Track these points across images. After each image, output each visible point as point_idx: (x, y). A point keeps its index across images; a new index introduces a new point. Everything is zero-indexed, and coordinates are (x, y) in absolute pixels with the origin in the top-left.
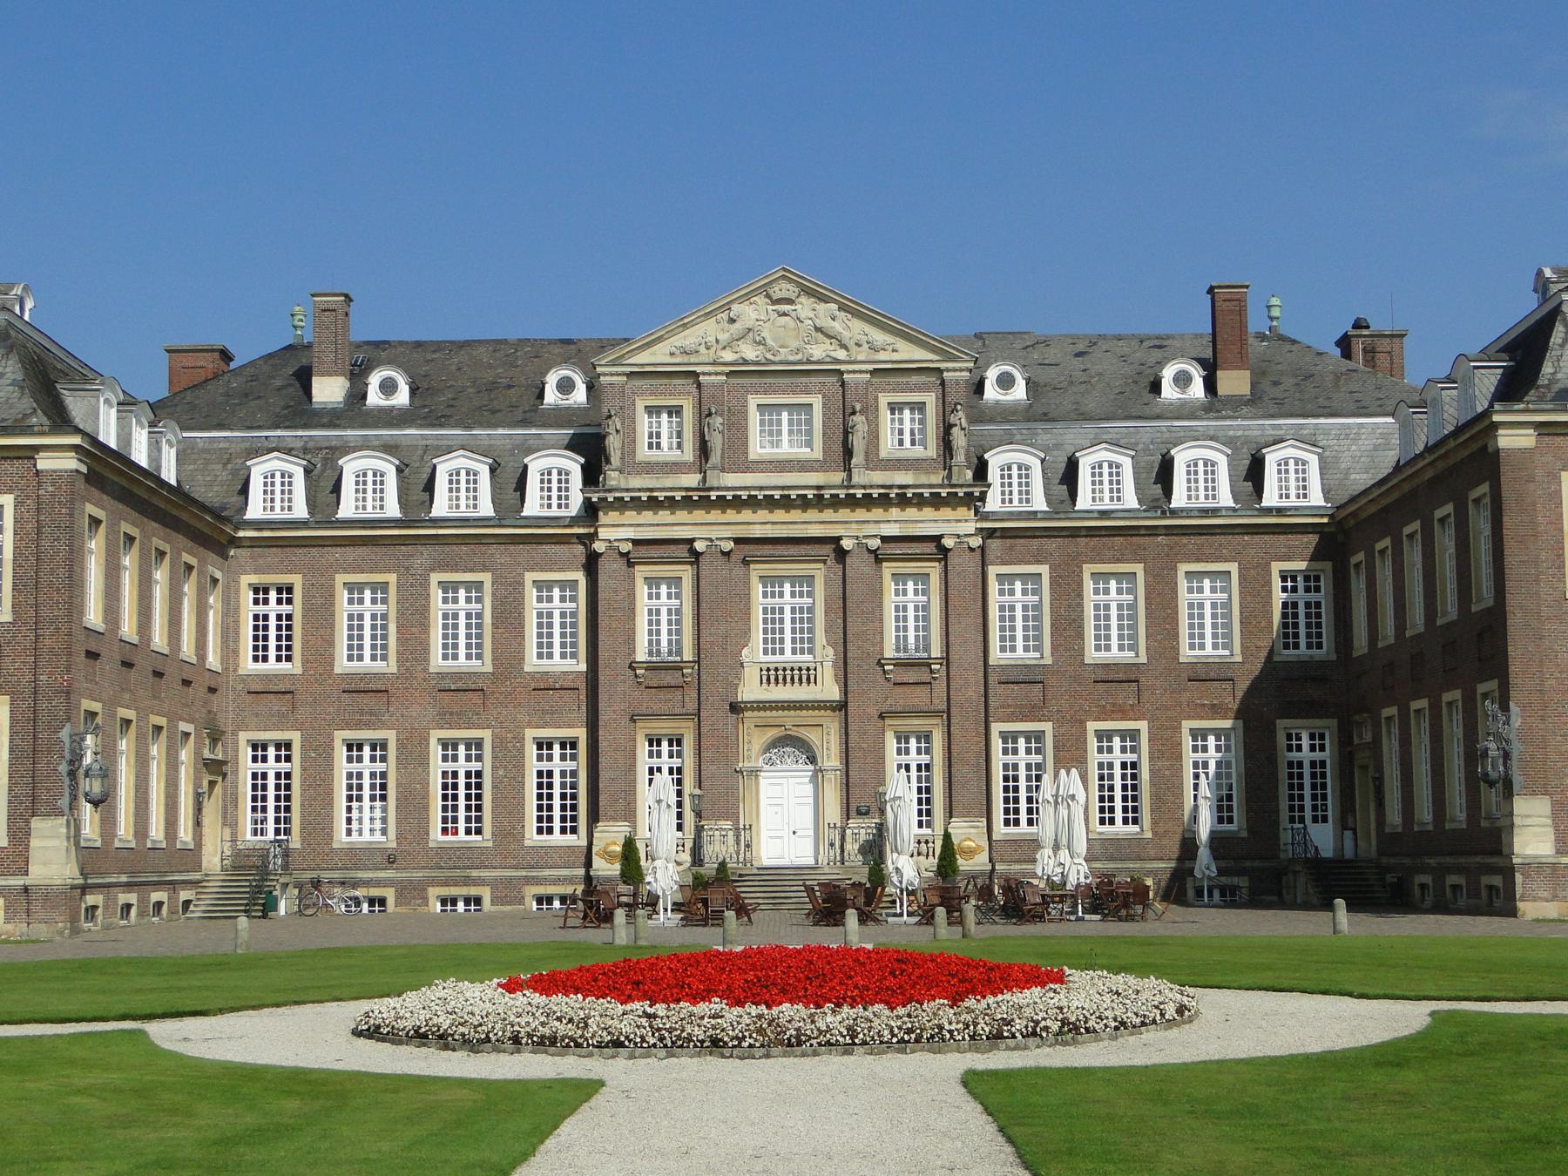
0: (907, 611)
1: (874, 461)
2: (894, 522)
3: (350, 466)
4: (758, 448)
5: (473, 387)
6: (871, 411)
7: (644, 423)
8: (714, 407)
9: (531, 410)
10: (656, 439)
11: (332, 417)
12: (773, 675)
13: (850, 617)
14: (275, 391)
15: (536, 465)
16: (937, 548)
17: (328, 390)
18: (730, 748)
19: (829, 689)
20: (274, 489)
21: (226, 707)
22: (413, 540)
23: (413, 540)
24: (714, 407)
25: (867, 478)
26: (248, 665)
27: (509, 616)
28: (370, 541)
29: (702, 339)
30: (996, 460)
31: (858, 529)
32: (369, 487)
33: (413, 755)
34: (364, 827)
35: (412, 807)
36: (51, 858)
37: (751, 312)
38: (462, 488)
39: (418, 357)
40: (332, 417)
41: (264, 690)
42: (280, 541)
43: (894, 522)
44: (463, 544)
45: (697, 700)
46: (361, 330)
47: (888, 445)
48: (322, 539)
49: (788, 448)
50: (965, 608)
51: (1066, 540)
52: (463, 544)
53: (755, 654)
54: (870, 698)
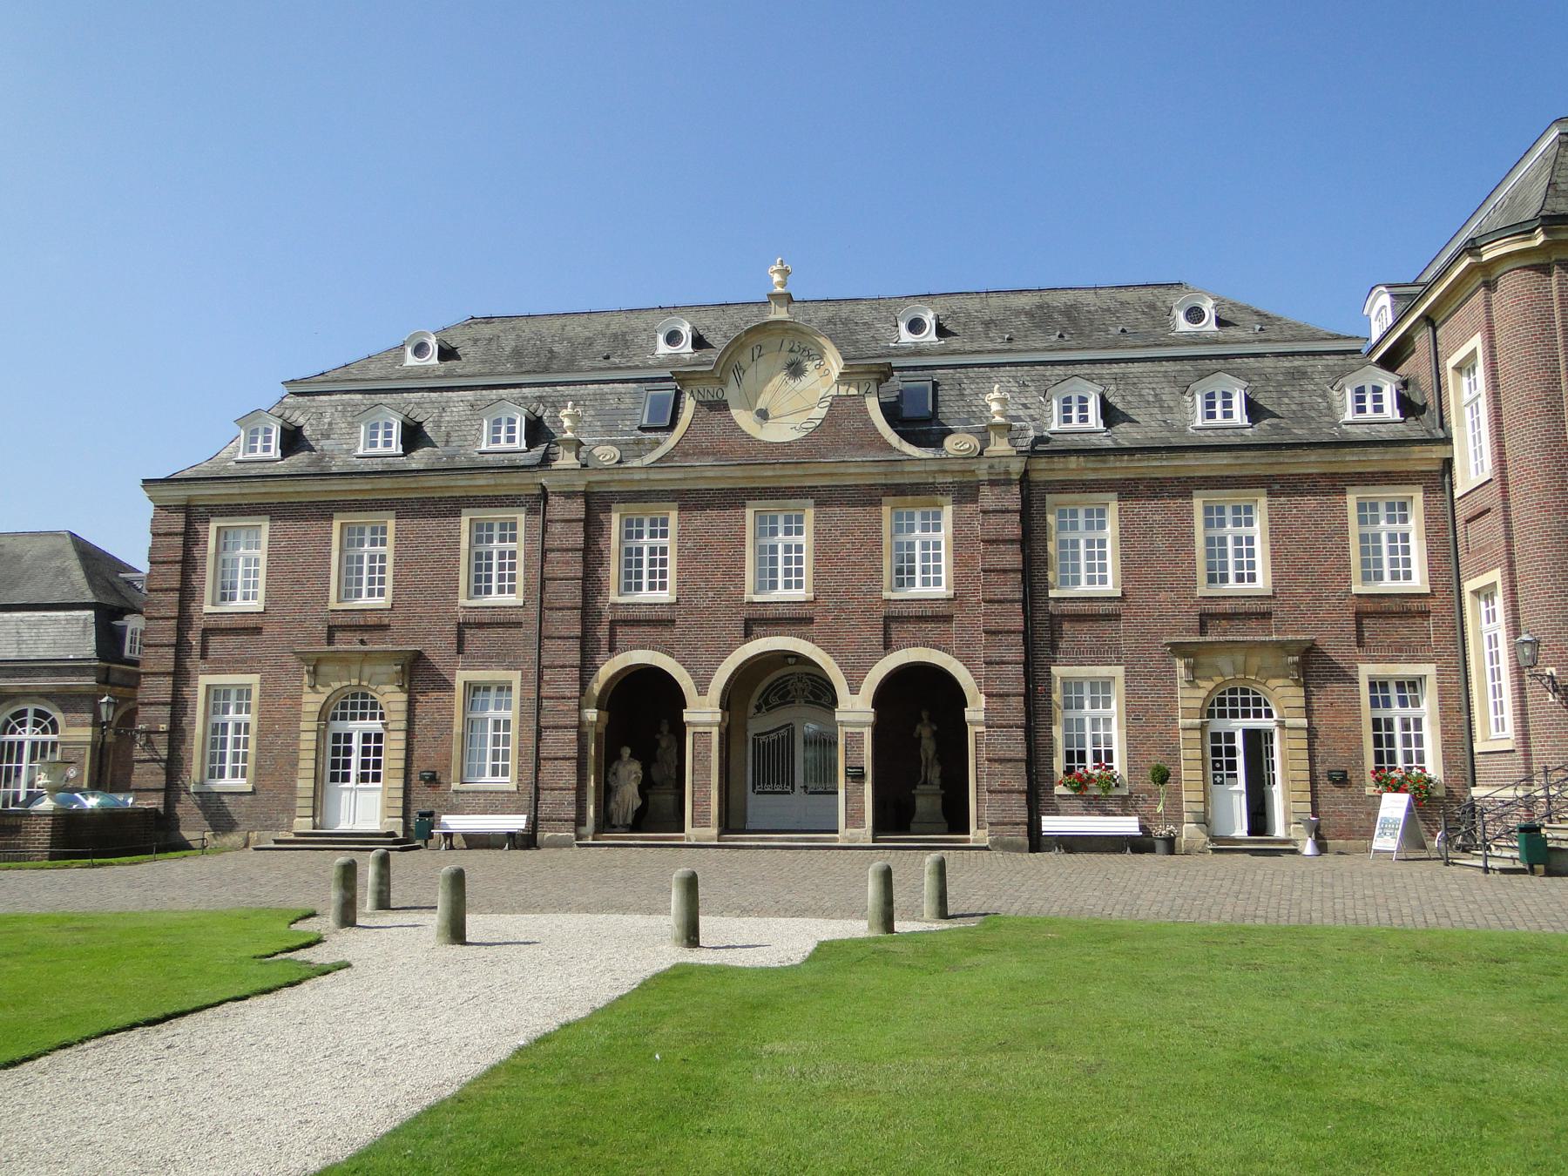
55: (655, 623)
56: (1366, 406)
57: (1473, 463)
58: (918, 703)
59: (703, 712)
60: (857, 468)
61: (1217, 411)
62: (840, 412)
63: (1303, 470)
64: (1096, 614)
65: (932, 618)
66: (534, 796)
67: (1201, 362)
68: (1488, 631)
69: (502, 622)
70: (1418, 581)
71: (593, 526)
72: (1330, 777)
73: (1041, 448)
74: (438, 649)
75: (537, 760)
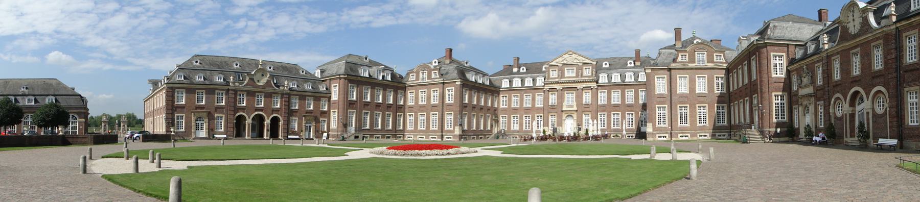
0: (587, 97)
1: (582, 76)
2: (585, 85)
3: (514, 80)
4: (566, 75)
5: (534, 69)
6: (582, 69)
7: (551, 73)
8: (561, 69)
9: (541, 72)
10: (554, 74)
11: (515, 74)
12: (568, 106)
13: (579, 98)
14: (507, 71)
15: (538, 79)
16: (590, 88)
17: (515, 70)
18: (561, 117)
19: (575, 108)
20: (505, 84)
21: (499, 112)
22: (522, 89)
23: (522, 89)
24: (561, 69)
25: (580, 79)
26: (501, 106)
27: (534, 99)
28: (517, 90)
29: (560, 61)
30: (601, 75)
31: (580, 86)
32: (517, 83)
33: (521, 118)
34: (515, 127)
35: (521, 125)
36: (457, 131)
37: (565, 56)
38: (529, 83)
39: (524, 65)
40: (515, 74)
41: (504, 110)
42: (506, 90)
43: (585, 85)
44: (528, 90)
45: (557, 110)
46: (521, 62)
47: (585, 74)
48: (511, 90)
49: (571, 75)
50: (595, 97)
51: (610, 86)
52: (528, 90)
53: (565, 103)
54: (583, 109)
55: (243, 109)
56: (322, 88)
57: (335, 97)
58: (275, 121)
59: (249, 121)
60: (270, 90)
61: (308, 87)
62: (268, 82)
63: (318, 97)
64: (296, 111)
65: (277, 111)
66: (226, 133)
67: (306, 80)
68: (334, 116)
69: (222, 108)
70: (326, 109)
71: (236, 94)
72: (317, 131)
73: (290, 89)
74: (212, 111)
75: (226, 127)
